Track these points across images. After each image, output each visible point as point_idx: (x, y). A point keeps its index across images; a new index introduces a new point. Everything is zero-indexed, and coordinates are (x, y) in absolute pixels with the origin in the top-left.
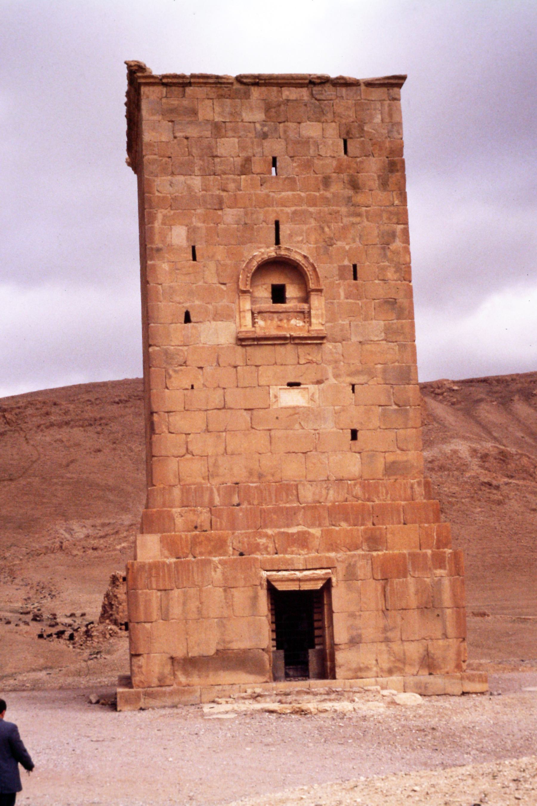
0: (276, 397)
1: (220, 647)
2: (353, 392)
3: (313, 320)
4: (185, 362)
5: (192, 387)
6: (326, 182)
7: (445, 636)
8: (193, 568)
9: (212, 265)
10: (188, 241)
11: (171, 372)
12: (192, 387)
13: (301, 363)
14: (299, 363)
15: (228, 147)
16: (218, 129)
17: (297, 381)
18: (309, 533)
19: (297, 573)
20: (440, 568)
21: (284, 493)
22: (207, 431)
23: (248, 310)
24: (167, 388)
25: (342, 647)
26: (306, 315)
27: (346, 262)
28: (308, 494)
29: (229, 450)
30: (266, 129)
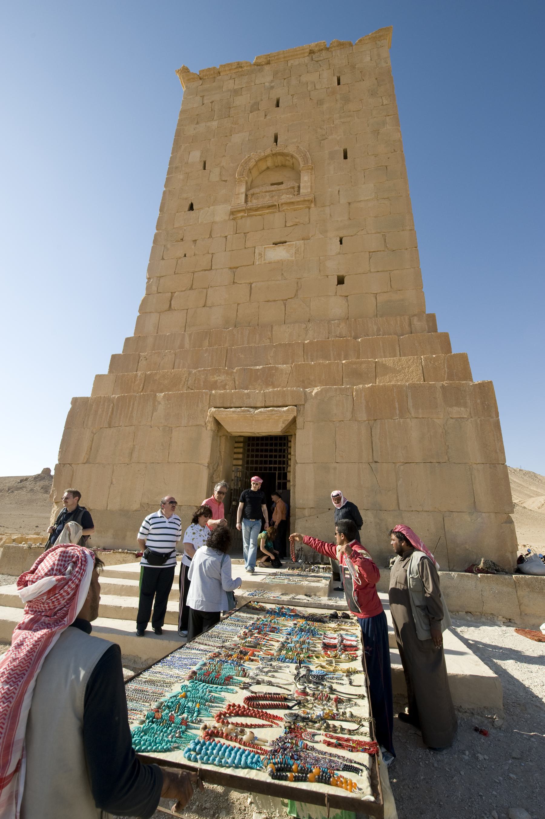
0: (260, 254)
1: (146, 501)
2: (341, 243)
3: (301, 191)
4: (182, 239)
5: (185, 256)
6: (320, 102)
7: (475, 508)
8: (133, 404)
9: (217, 171)
10: (200, 158)
11: (169, 246)
12: (185, 256)
13: (287, 225)
14: (286, 226)
15: (242, 101)
16: (236, 92)
17: (283, 240)
18: (277, 369)
19: (251, 410)
20: (458, 404)
21: (257, 336)
22: (191, 288)
23: (242, 193)
24: (163, 259)
25: (306, 512)
26: (296, 189)
27: (337, 148)
28: (284, 334)
29: (209, 303)
30: (273, 84)
